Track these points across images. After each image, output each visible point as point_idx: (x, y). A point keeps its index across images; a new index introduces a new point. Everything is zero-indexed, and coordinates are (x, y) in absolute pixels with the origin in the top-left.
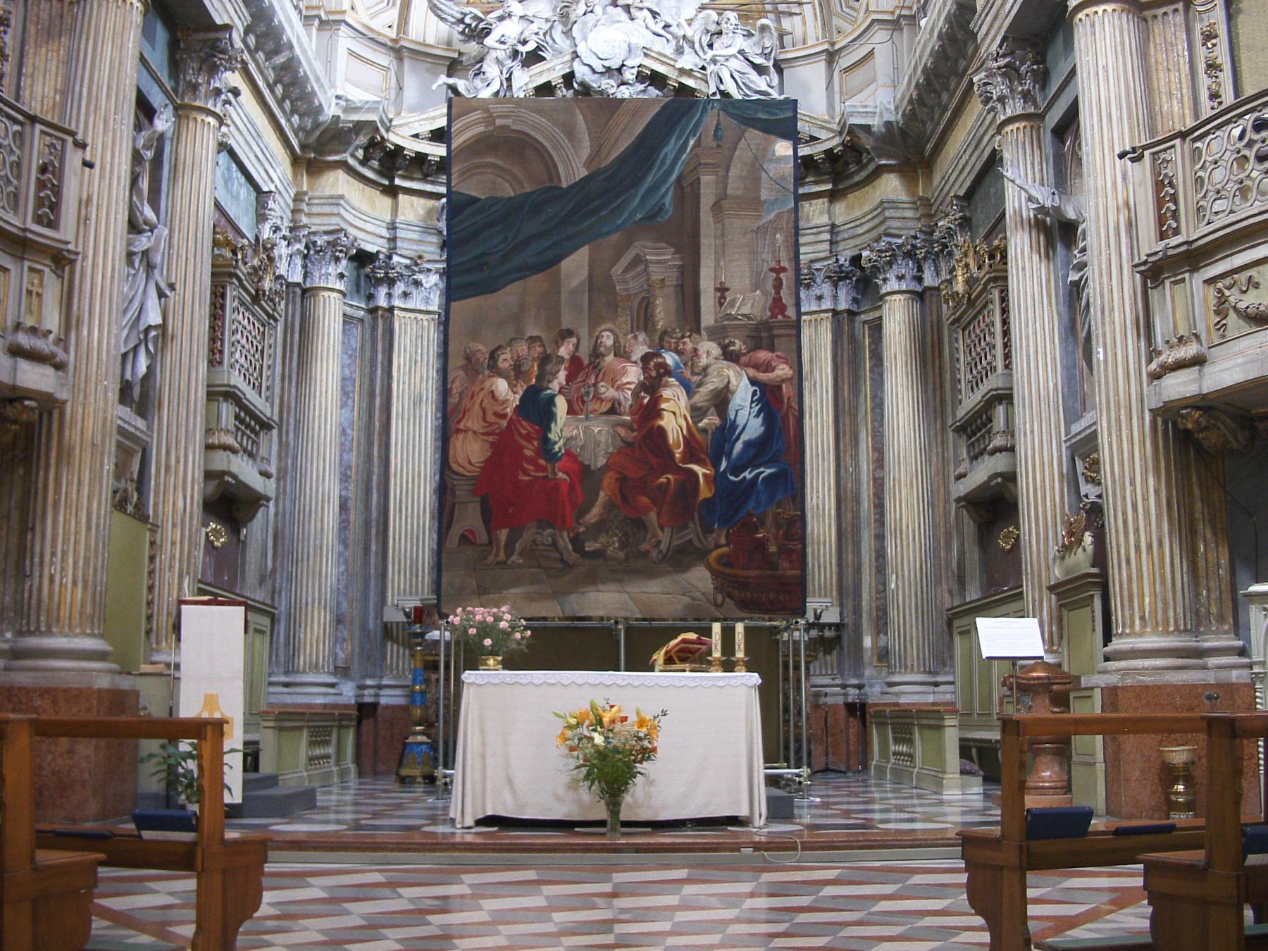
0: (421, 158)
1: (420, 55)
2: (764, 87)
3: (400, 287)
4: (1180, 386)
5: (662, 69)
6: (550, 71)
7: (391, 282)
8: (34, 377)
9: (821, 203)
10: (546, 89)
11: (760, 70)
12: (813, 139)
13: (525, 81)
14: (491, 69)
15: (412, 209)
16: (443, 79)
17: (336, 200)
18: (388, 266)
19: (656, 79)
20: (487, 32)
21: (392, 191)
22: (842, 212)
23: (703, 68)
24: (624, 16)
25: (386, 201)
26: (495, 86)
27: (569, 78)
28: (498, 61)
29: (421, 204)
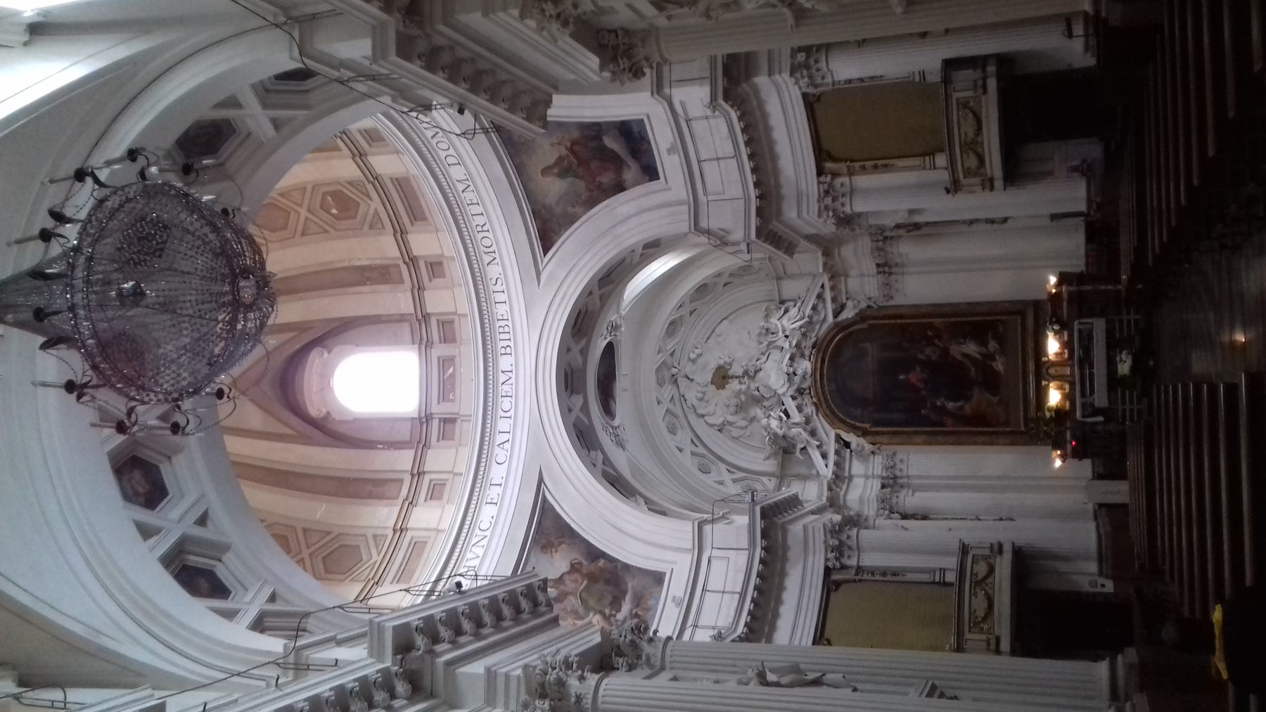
0: (836, 464)
1: (783, 466)
2: (796, 309)
3: (898, 473)
4: (999, 184)
5: (788, 356)
6: (791, 405)
7: (895, 478)
8: (1007, 548)
9: (849, 280)
10: (800, 409)
11: (786, 311)
12: (823, 286)
13: (797, 417)
14: (794, 431)
15: (857, 468)
16: (798, 454)
17: (861, 499)
18: (888, 478)
19: (792, 359)
20: (775, 434)
21: (851, 478)
22: (853, 272)
23: (787, 337)
24: (761, 374)
25: (856, 480)
26: (800, 430)
27: (794, 398)
28: (790, 428)
29: (856, 463)
